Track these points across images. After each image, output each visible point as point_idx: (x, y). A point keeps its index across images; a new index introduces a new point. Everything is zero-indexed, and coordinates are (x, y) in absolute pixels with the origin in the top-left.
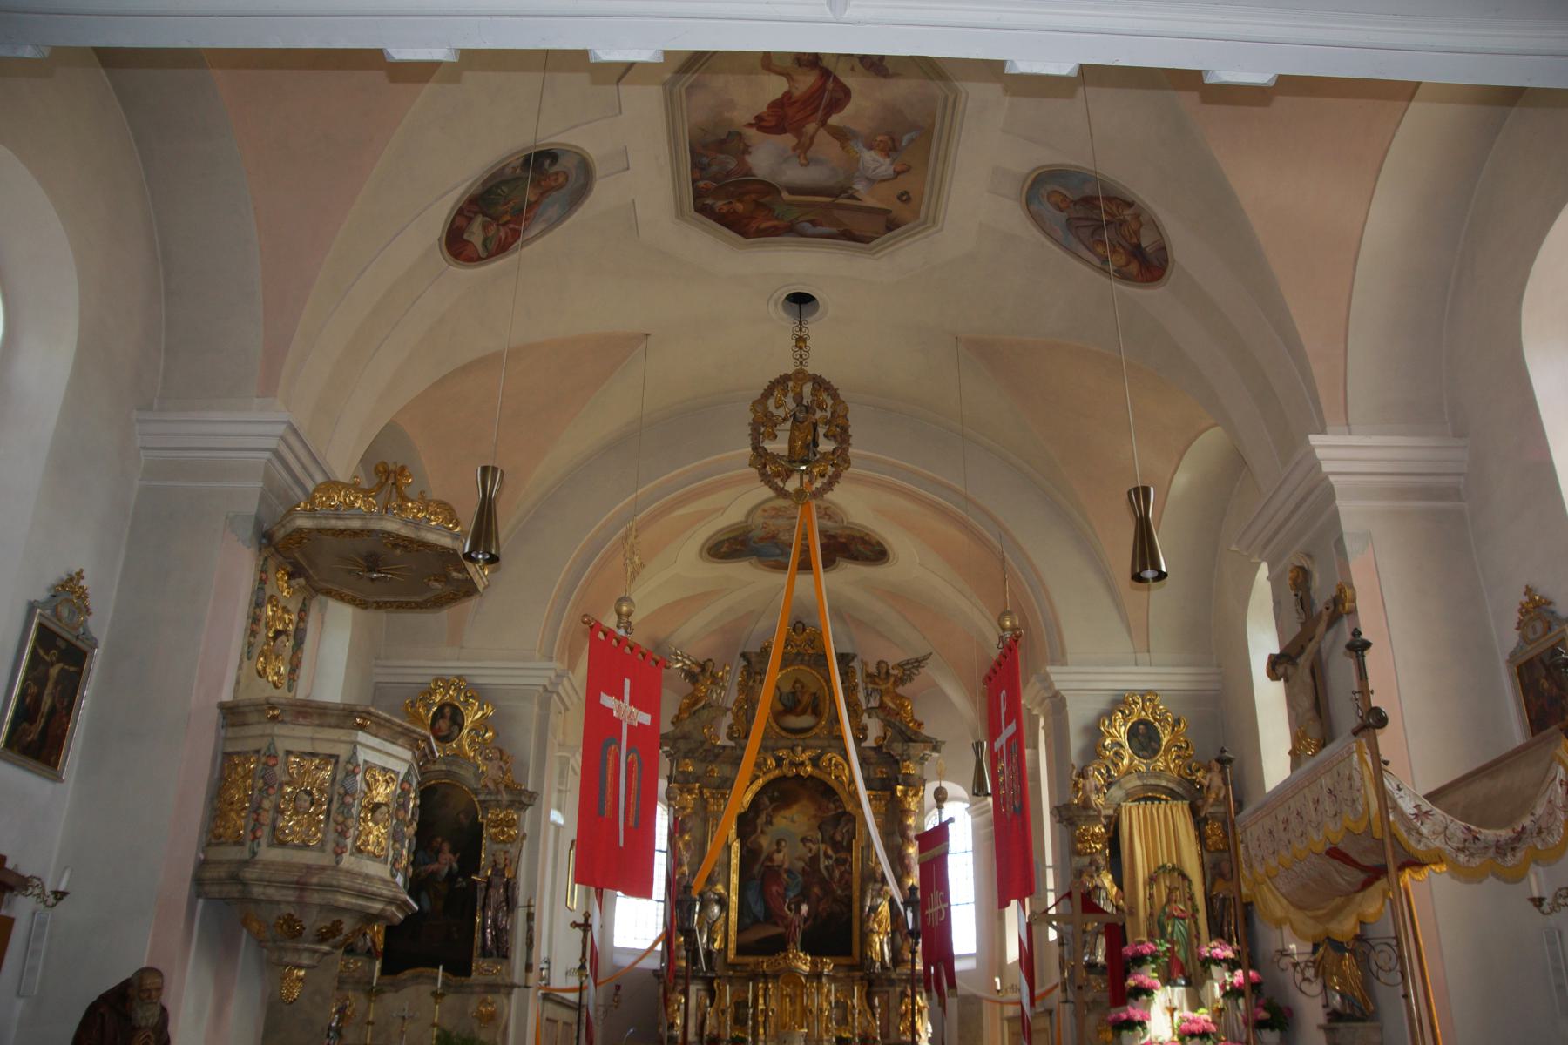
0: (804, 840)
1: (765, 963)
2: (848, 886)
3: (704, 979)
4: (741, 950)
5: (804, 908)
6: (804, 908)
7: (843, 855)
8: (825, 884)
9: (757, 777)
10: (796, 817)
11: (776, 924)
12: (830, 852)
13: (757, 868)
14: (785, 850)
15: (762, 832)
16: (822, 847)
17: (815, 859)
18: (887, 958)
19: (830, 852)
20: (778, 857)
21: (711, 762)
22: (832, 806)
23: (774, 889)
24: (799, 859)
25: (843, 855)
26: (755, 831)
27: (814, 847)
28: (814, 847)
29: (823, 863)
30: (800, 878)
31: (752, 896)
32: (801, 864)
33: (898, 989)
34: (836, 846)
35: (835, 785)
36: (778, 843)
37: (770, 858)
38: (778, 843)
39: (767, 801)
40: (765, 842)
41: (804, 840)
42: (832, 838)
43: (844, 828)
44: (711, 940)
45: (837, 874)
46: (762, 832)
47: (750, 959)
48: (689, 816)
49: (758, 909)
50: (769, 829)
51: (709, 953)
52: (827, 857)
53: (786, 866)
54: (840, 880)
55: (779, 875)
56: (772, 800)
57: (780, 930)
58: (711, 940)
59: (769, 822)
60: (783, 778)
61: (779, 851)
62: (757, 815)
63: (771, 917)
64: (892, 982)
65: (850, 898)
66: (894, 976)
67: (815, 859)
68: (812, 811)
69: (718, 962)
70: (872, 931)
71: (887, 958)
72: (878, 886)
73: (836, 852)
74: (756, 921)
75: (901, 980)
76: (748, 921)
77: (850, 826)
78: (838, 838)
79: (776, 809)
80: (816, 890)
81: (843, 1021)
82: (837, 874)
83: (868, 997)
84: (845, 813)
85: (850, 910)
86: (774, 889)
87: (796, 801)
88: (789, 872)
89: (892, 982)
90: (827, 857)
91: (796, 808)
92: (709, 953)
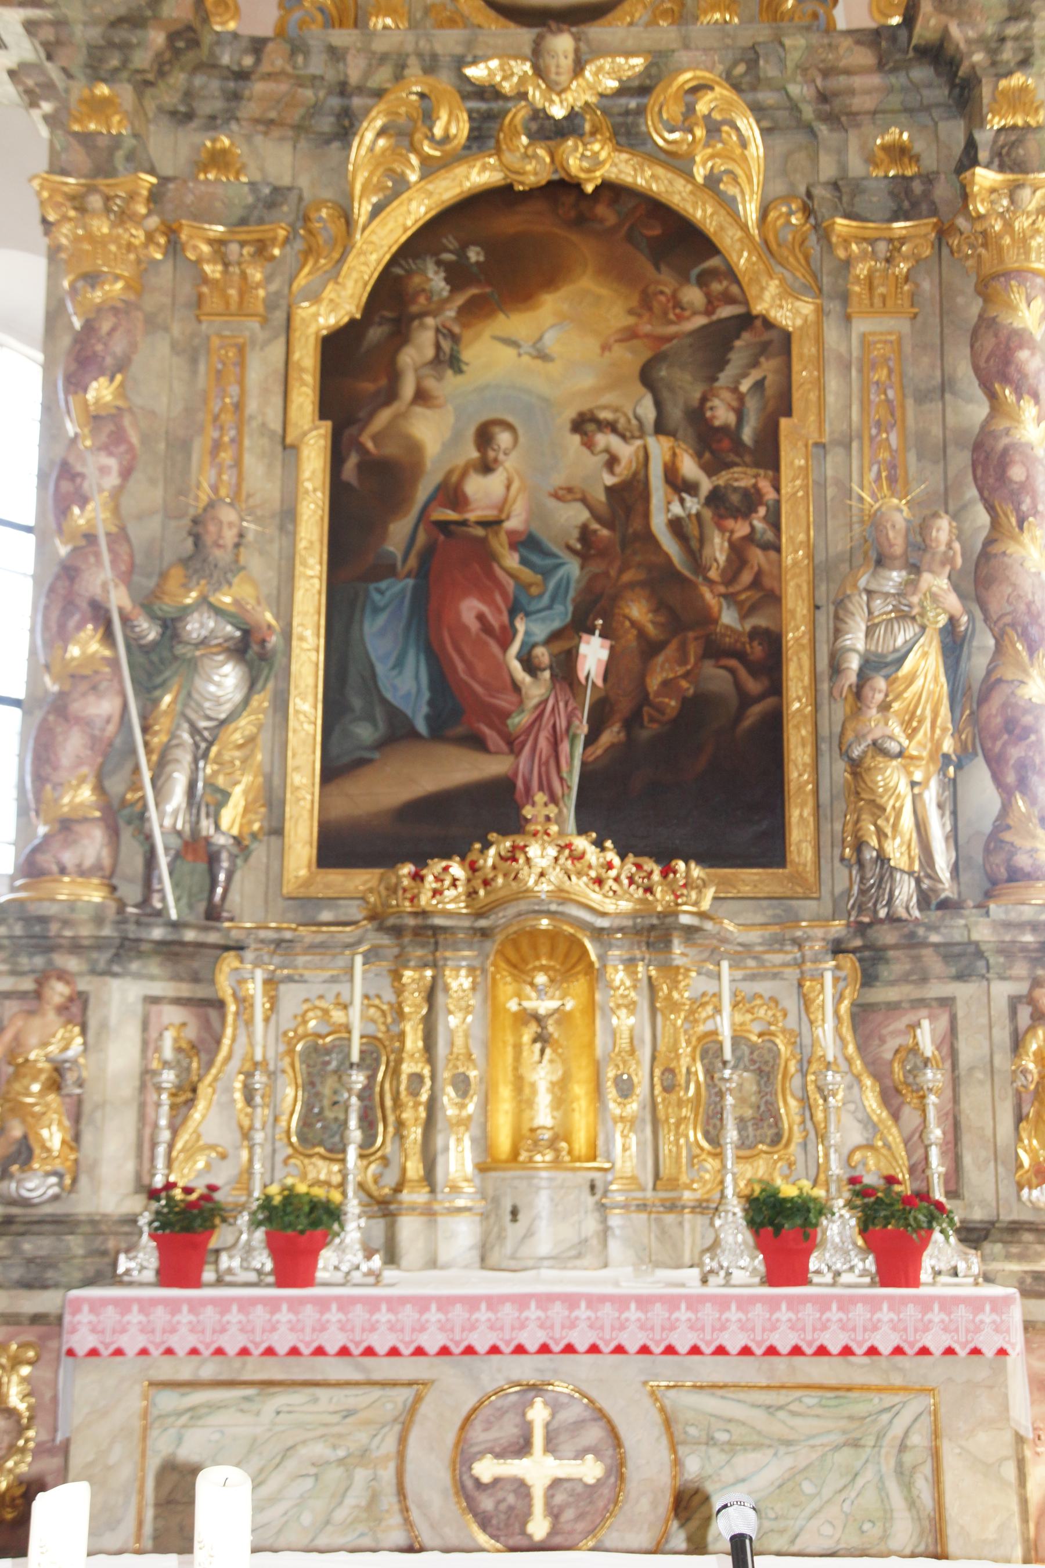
0: (584, 424)
1: (445, 888)
2: (767, 596)
3: (171, 951)
4: (337, 848)
5: (593, 654)
6: (593, 654)
7: (741, 477)
8: (670, 588)
9: (400, 187)
10: (551, 341)
11: (477, 743)
12: (689, 467)
13: (399, 532)
14: (510, 463)
15: (422, 397)
16: (659, 448)
17: (628, 498)
18: (942, 860)
19: (689, 467)
20: (483, 491)
21: (212, 123)
22: (693, 295)
23: (470, 609)
24: (565, 494)
25: (741, 477)
26: (391, 395)
27: (626, 451)
28: (626, 451)
29: (663, 509)
30: (573, 568)
31: (380, 638)
32: (576, 515)
33: (1002, 991)
34: (714, 444)
35: (702, 213)
36: (484, 437)
37: (451, 493)
38: (484, 437)
39: (437, 281)
40: (434, 435)
41: (584, 424)
42: (697, 416)
43: (743, 375)
44: (206, 800)
45: (718, 550)
46: (422, 397)
47: (361, 880)
48: (120, 310)
49: (406, 686)
50: (449, 386)
51: (198, 852)
52: (679, 485)
53: (515, 523)
54: (731, 575)
55: (487, 557)
56: (458, 275)
57: (492, 766)
58: (206, 800)
59: (448, 360)
60: (500, 197)
61: (486, 467)
62: (401, 333)
63: (458, 714)
64: (966, 960)
65: (773, 642)
66: (983, 933)
67: (628, 498)
68: (615, 312)
69: (244, 897)
70: (878, 748)
71: (942, 860)
72: (896, 576)
73: (710, 470)
74: (398, 733)
75: (1008, 951)
76: (365, 733)
77: (768, 368)
78: (722, 414)
79: (475, 311)
80: (638, 610)
81: (765, 1128)
82: (718, 550)
83: (863, 1018)
84: (747, 320)
85: (776, 688)
86: (470, 609)
87: (551, 280)
88: (528, 543)
89: (966, 960)
90: (679, 485)
91: (551, 304)
92: (198, 852)
